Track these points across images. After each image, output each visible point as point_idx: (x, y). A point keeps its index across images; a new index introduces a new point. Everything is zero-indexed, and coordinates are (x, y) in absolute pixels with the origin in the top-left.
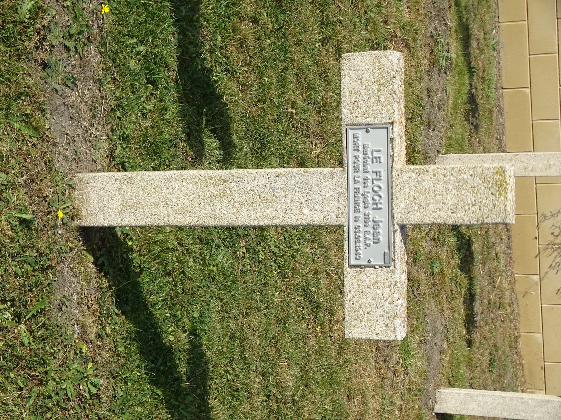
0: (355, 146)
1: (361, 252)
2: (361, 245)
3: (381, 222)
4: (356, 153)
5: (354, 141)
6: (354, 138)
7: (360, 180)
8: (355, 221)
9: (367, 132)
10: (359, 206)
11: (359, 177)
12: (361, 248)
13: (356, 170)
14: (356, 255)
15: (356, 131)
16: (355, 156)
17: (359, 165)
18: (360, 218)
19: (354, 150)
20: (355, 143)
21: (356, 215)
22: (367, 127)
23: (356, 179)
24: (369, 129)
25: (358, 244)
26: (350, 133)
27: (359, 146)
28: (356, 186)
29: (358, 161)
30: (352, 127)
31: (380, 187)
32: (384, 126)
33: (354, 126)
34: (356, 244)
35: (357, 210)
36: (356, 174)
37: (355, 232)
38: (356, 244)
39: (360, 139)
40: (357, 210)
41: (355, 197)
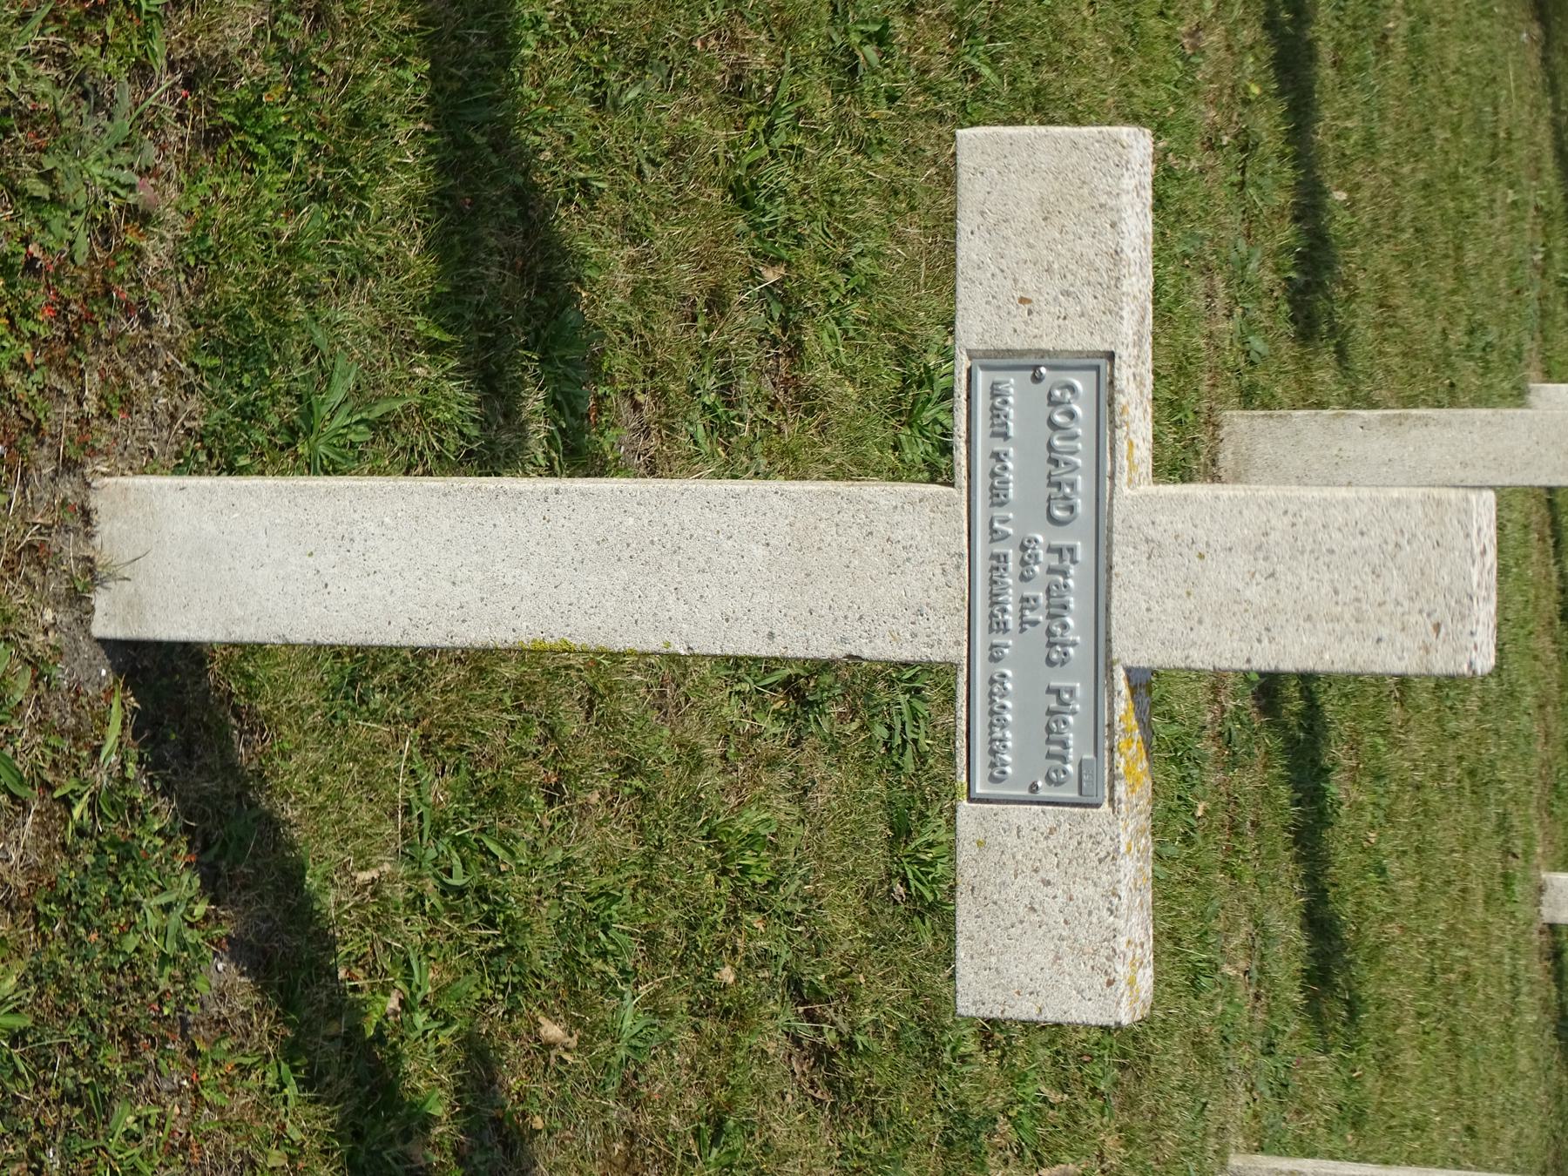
0: (996, 421)
1: (1007, 758)
2: (1008, 734)
3: (1074, 644)
4: (999, 445)
5: (993, 408)
6: (994, 395)
7: (1011, 531)
8: (993, 659)
9: (1037, 379)
10: (1004, 611)
11: (1005, 521)
12: (1009, 744)
13: (997, 497)
14: (993, 765)
15: (998, 376)
16: (996, 456)
17: (1007, 482)
18: (1006, 651)
19: (994, 435)
20: (995, 413)
21: (996, 641)
22: (1038, 362)
23: (996, 525)
24: (1043, 370)
25: (998, 734)
26: (981, 378)
27: (1010, 424)
28: (998, 549)
29: (1005, 468)
30: (985, 361)
31: (1072, 388)
32: (1088, 362)
33: (998, 359)
34: (991, 733)
35: (997, 626)
36: (999, 513)
37: (991, 694)
38: (991, 733)
39: (1011, 399)
40: (997, 626)
41: (993, 582)
